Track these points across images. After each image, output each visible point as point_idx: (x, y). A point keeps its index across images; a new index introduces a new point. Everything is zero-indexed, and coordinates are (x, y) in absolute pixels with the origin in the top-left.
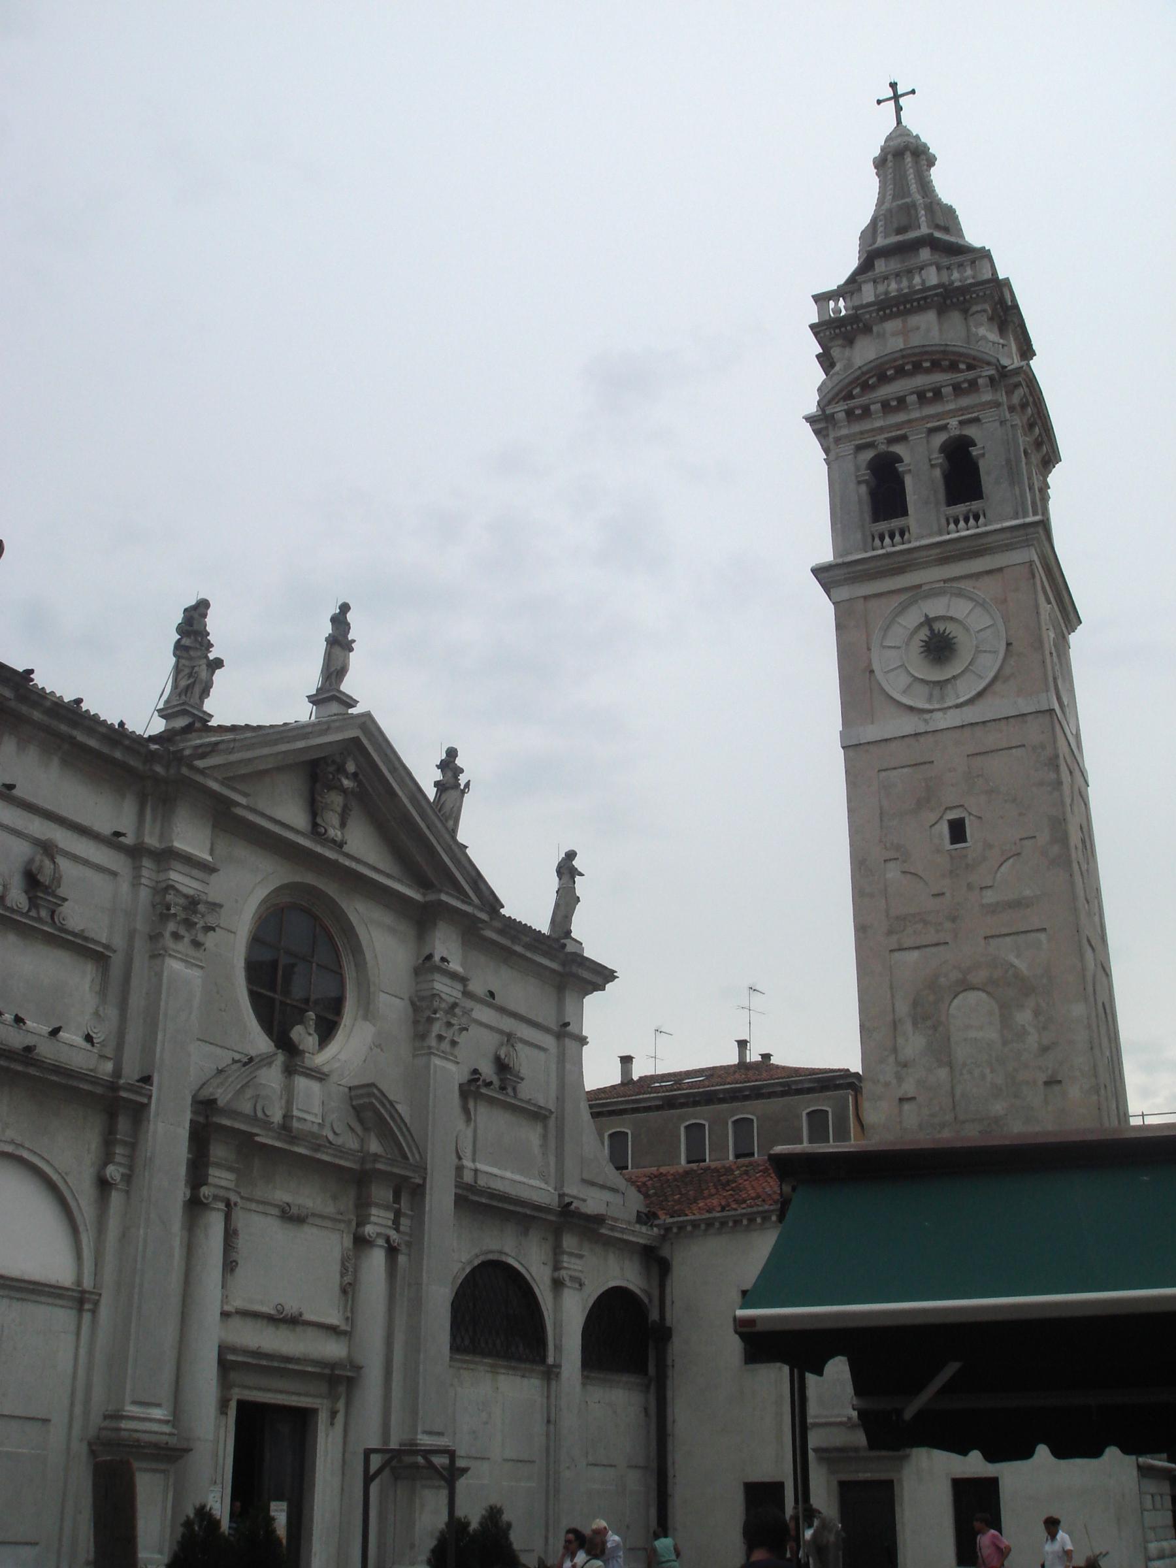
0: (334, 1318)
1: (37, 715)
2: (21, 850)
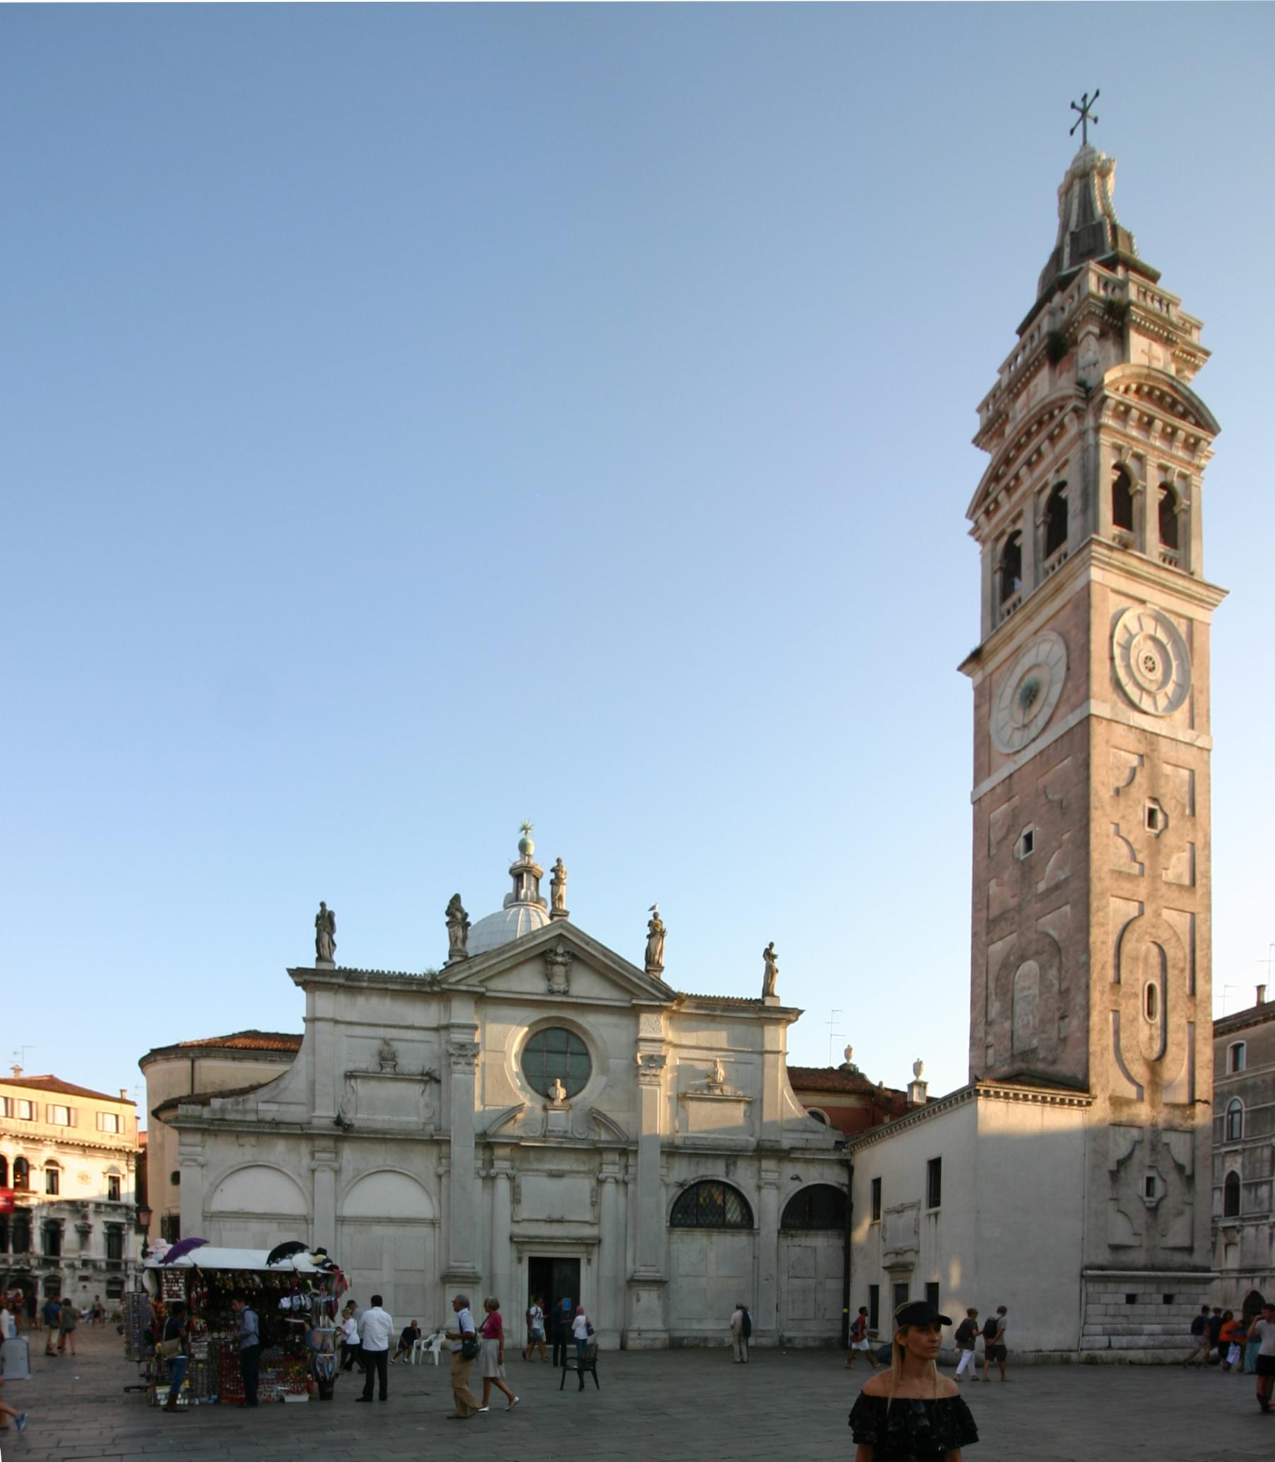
0: (588, 1218)
1: (365, 984)
2: (376, 1045)
